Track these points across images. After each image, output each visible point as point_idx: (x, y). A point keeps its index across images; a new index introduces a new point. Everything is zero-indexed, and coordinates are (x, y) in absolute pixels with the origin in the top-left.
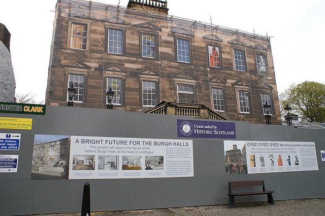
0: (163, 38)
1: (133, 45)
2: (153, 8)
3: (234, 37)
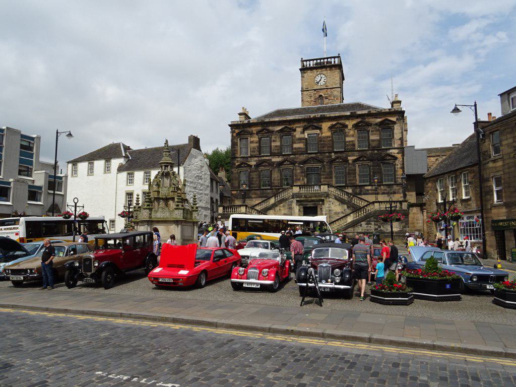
0: (297, 136)
1: (276, 146)
2: (324, 70)
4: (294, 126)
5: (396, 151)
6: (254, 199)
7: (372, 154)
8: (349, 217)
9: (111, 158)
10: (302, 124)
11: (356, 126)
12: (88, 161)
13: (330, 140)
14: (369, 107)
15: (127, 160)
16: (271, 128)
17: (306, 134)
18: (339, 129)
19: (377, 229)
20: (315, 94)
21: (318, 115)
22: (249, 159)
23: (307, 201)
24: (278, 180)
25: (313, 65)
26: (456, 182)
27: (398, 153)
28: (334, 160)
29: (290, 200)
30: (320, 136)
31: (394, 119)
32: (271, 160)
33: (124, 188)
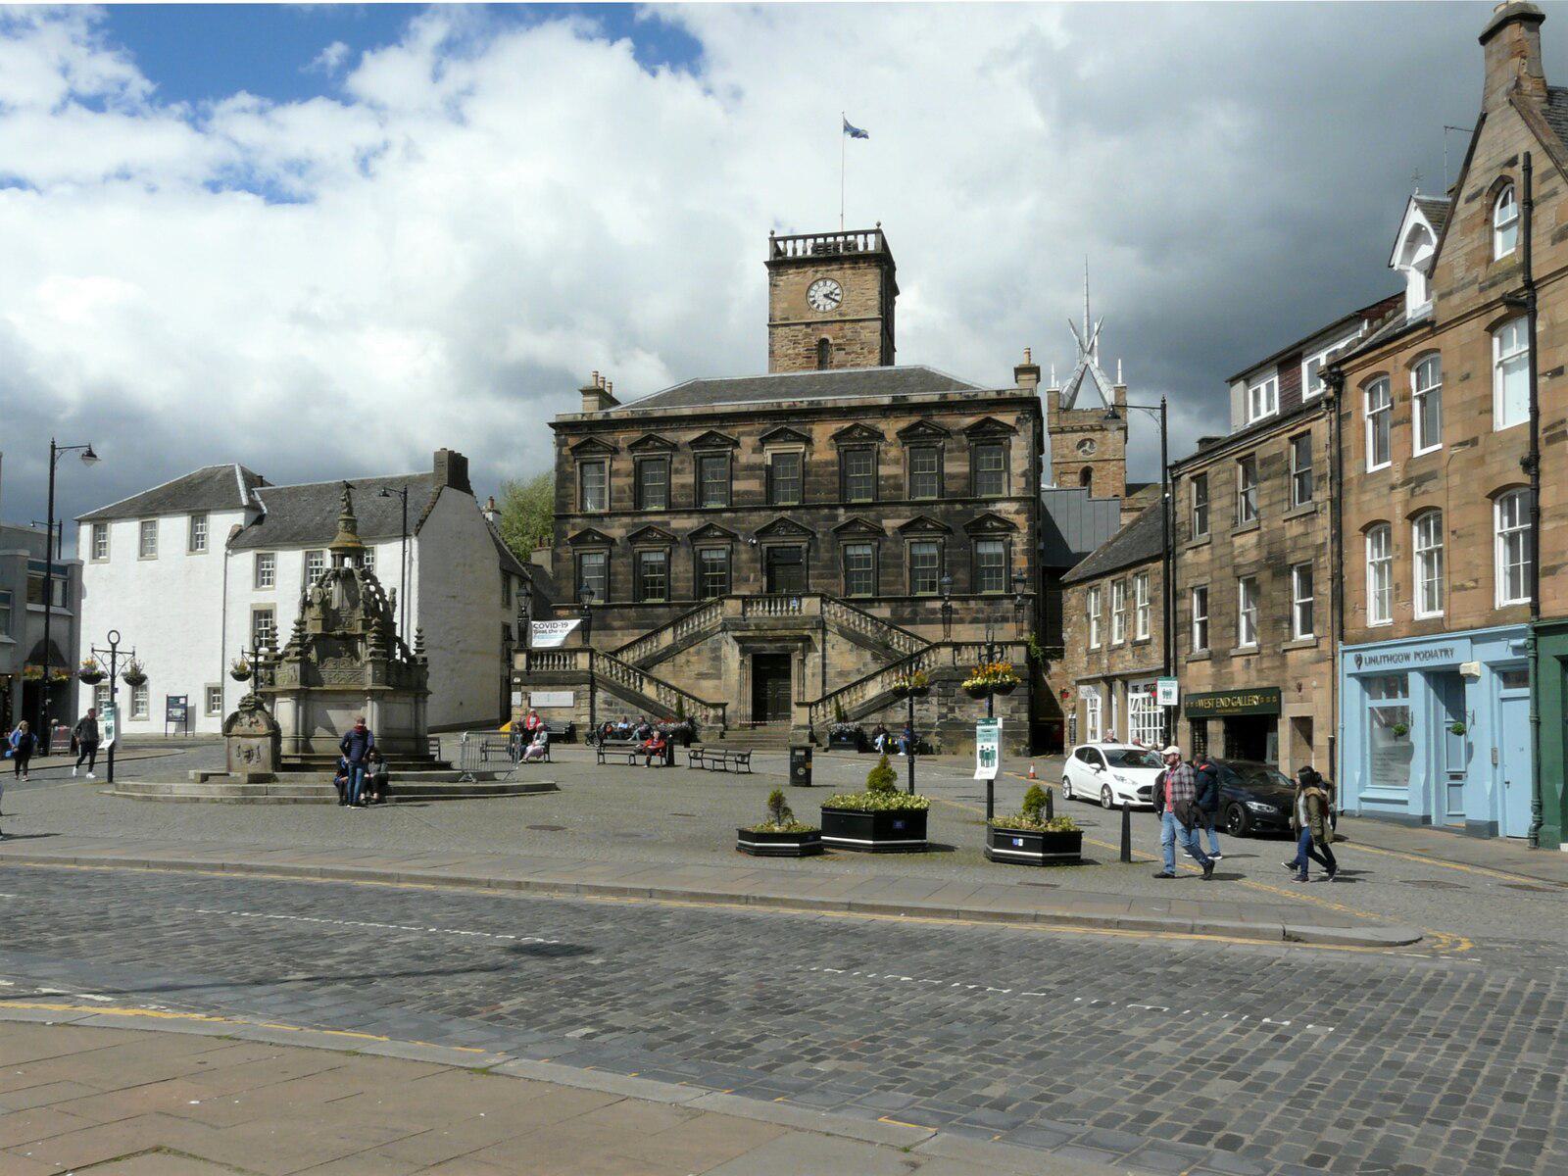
1: (683, 486)
3: (914, 419)
4: (733, 431)
5: (1013, 507)
6: (619, 633)
7: (946, 515)
8: (871, 684)
9: (207, 511)
10: (758, 426)
11: (905, 435)
12: (140, 517)
13: (833, 472)
14: (947, 383)
15: (254, 516)
16: (669, 436)
17: (769, 454)
18: (857, 443)
19: (946, 717)
20: (807, 335)
21: (803, 401)
22: (606, 519)
23: (764, 639)
24: (688, 580)
25: (805, 252)
26: (1126, 598)
27: (1017, 512)
28: (845, 527)
29: (716, 637)
30: (807, 459)
31: (1008, 418)
32: (668, 524)
33: (246, 597)
